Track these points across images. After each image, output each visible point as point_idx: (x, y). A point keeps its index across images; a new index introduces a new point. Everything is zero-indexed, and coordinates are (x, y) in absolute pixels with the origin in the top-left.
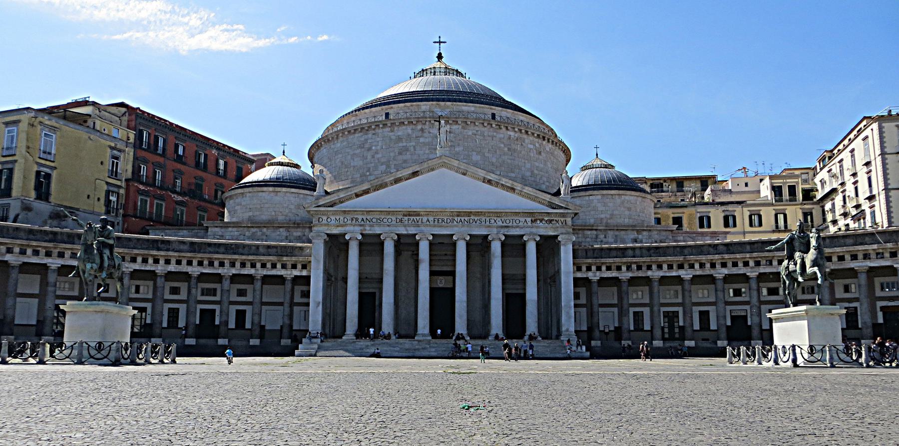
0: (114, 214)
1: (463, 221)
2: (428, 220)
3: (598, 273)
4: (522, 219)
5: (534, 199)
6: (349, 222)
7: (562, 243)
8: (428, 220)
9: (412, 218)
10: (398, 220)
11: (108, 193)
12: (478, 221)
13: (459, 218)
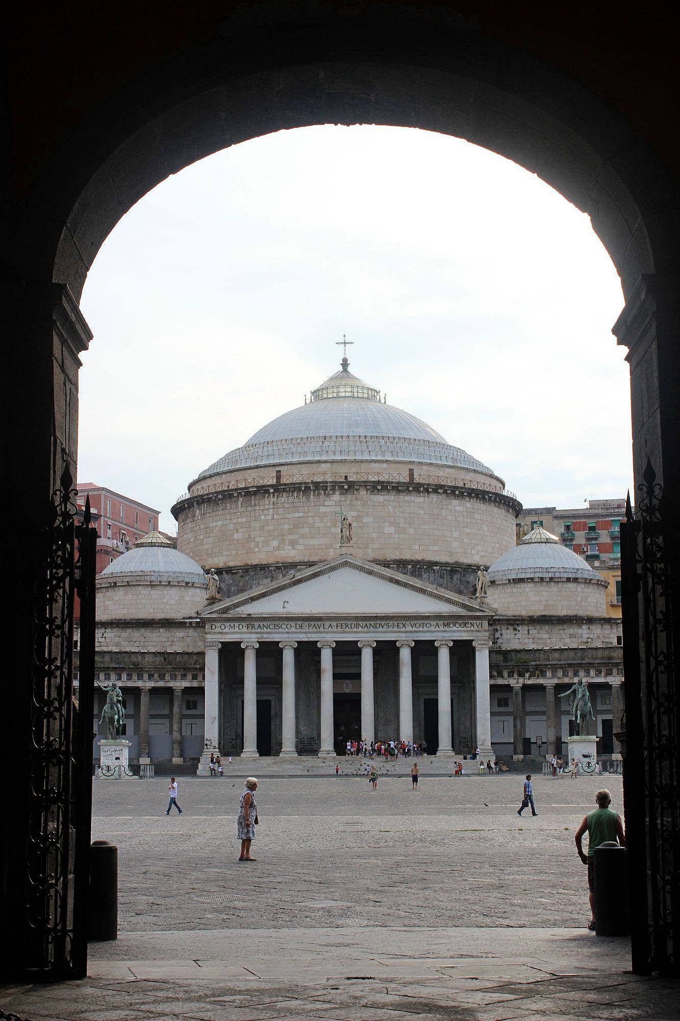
2: (330, 626)
3: (521, 680)
4: (434, 623)
5: (448, 601)
6: (245, 629)
7: (476, 649)
8: (330, 626)
9: (312, 623)
10: (298, 626)
12: (385, 626)
13: (364, 623)
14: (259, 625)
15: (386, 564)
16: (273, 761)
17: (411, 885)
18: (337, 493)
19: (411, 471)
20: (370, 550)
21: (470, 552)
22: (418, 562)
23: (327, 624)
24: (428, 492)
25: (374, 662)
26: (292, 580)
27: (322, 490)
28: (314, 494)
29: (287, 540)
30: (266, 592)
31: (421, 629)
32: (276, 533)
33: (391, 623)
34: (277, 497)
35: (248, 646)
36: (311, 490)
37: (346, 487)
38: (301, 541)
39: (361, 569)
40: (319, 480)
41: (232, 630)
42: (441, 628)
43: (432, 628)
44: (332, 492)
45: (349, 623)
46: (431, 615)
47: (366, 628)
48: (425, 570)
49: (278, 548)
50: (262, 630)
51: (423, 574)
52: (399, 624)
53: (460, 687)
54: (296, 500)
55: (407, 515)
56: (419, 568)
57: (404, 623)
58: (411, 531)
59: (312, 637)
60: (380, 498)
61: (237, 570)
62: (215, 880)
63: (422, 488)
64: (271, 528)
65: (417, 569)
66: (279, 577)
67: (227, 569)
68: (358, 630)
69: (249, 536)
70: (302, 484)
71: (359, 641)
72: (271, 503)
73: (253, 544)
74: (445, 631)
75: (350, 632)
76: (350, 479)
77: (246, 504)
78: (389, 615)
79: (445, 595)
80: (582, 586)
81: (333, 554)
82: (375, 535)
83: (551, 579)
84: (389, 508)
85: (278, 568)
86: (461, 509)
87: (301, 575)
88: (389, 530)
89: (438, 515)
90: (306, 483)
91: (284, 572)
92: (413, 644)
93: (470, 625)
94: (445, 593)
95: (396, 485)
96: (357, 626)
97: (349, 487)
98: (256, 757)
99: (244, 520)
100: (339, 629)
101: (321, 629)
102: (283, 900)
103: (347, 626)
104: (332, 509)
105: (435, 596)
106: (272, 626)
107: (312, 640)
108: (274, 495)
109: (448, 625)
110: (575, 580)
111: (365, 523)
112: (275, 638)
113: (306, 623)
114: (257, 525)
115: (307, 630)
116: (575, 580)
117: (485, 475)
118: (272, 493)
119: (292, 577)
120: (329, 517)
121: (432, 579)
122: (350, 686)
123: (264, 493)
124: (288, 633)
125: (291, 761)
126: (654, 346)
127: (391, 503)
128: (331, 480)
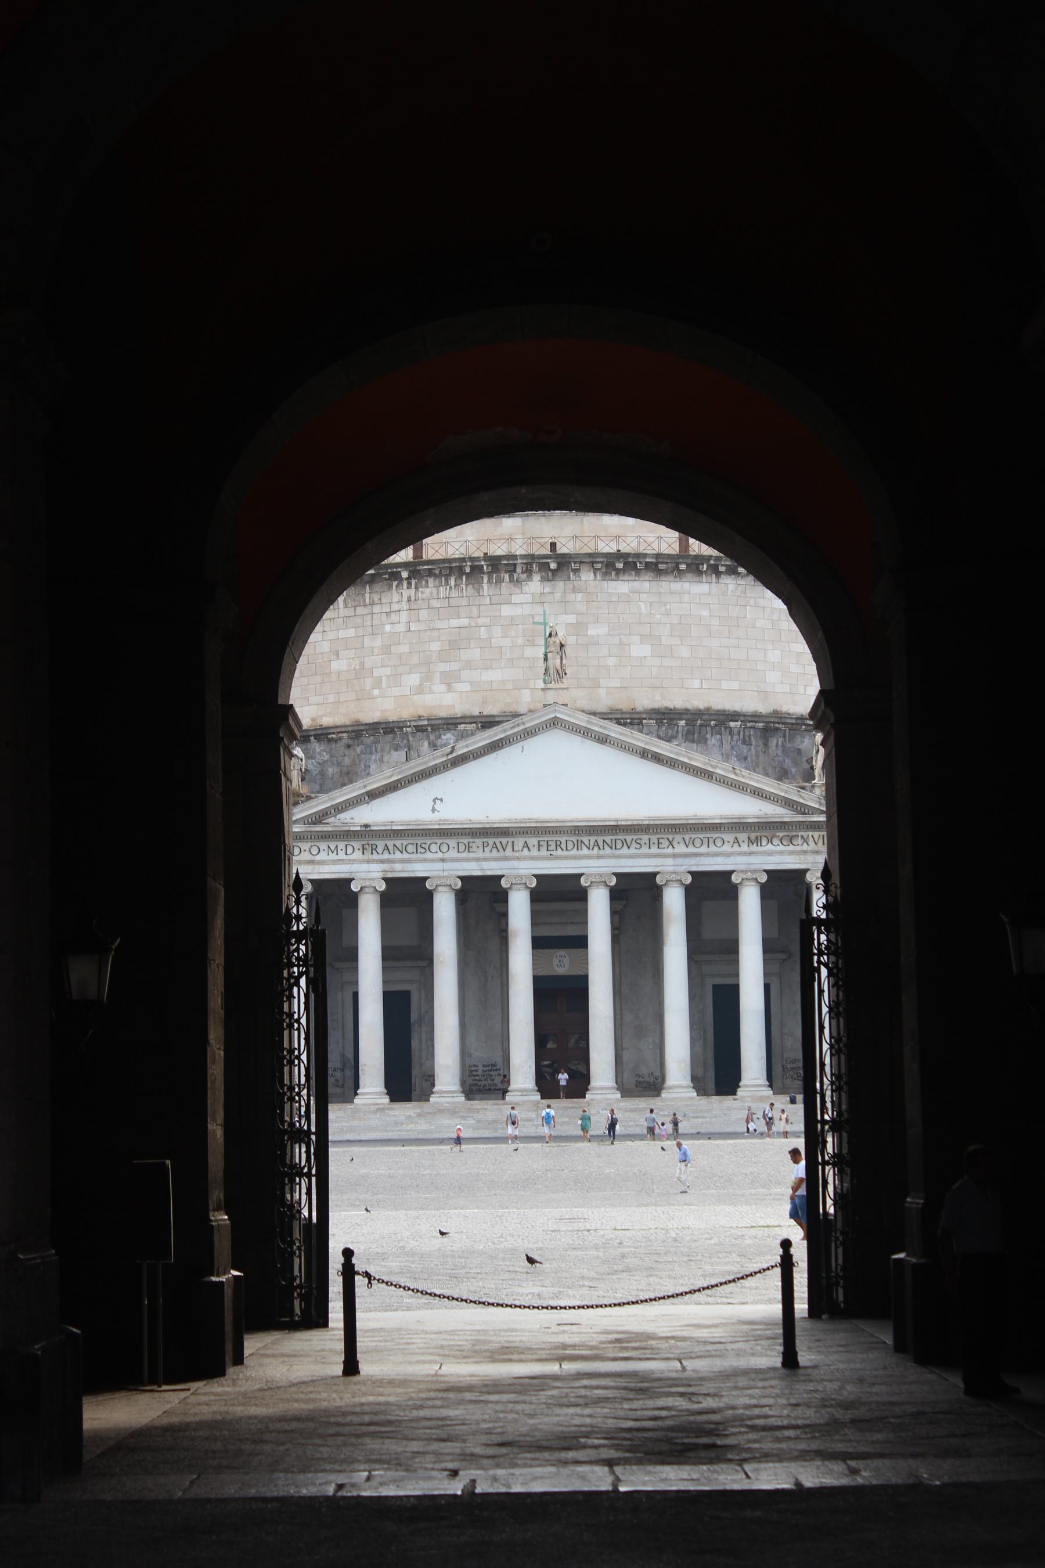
1: (601, 843)
4: (729, 837)
5: (758, 793)
6: (358, 855)
8: (526, 845)
9: (491, 841)
10: (462, 847)
13: (593, 839)
14: (386, 845)
15: (631, 719)
16: (418, 1111)
17: (634, 1273)
18: (536, 577)
20: (602, 692)
21: (802, 692)
22: (698, 714)
23: (520, 842)
24: (718, 574)
25: (614, 913)
26: (450, 757)
27: (507, 571)
28: (489, 582)
29: (438, 674)
30: (398, 780)
32: (415, 660)
33: (645, 838)
34: (416, 588)
35: (365, 887)
36: (484, 573)
37: (553, 566)
38: (465, 674)
39: (585, 733)
40: (499, 552)
41: (333, 856)
42: (745, 847)
43: (726, 848)
44: (525, 575)
45: (563, 840)
46: (724, 821)
47: (596, 848)
48: (713, 728)
49: (420, 690)
50: (392, 856)
51: (708, 736)
52: (660, 841)
53: (784, 960)
54: (454, 593)
55: (675, 620)
56: (701, 725)
57: (670, 837)
58: (684, 652)
59: (491, 868)
60: (622, 586)
61: (338, 733)
62: (400, 1273)
63: (705, 566)
64: (405, 649)
65: (697, 729)
66: (422, 746)
67: (319, 732)
68: (580, 853)
69: (362, 664)
70: (465, 562)
71: (583, 874)
72: (405, 599)
73: (369, 682)
74: (751, 854)
75: (566, 858)
76: (561, 550)
77: (354, 600)
78: (640, 823)
79: (752, 783)
81: (529, 699)
82: (611, 662)
84: (640, 606)
85: (420, 729)
87: (467, 746)
88: (640, 650)
89: (737, 618)
90: (472, 559)
91: (432, 737)
92: (689, 880)
93: (800, 841)
94: (751, 779)
95: (653, 560)
96: (578, 845)
97: (560, 565)
98: (384, 1104)
99: (351, 633)
100: (544, 852)
101: (509, 852)
102: (486, 1286)
103: (558, 845)
104: (527, 610)
105: (731, 785)
106: (410, 848)
107: (489, 873)
108: (409, 584)
109: (758, 841)
111: (593, 636)
112: (417, 869)
113: (479, 841)
114: (378, 642)
115: (480, 854)
118: (406, 579)
119: (449, 750)
120: (520, 626)
121: (727, 747)
122: (566, 961)
123: (389, 579)
124: (443, 860)
125: (452, 1112)
126: (833, 753)
127: (644, 596)
128: (523, 552)
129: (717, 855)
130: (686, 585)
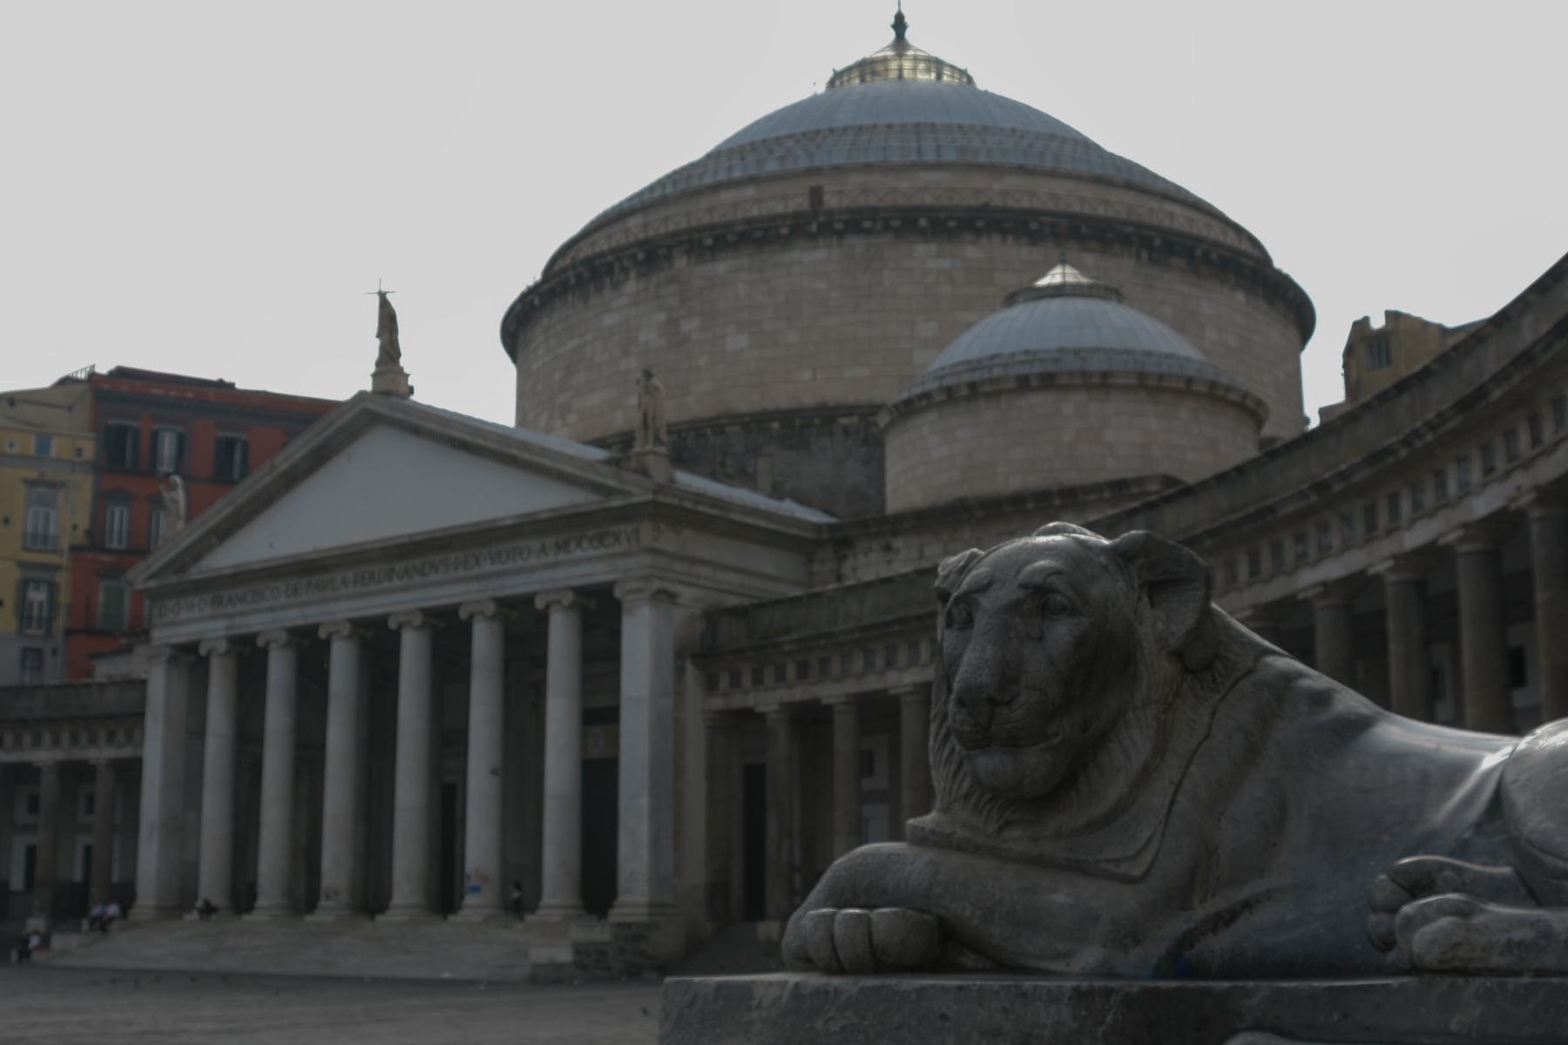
0: (41, 632)
4: (535, 544)
6: (208, 611)
7: (625, 606)
8: (344, 583)
11: (24, 586)
19: (816, 194)
24: (840, 235)
31: (510, 565)
43: (533, 561)
74: (555, 565)
80: (1081, 397)
83: (973, 386)
86: (946, 264)
88: (736, 341)
109: (562, 547)
110: (1048, 381)
116: (1048, 381)
117: (1128, 186)
124: (272, 609)
129: (520, 571)
130: (796, 254)
